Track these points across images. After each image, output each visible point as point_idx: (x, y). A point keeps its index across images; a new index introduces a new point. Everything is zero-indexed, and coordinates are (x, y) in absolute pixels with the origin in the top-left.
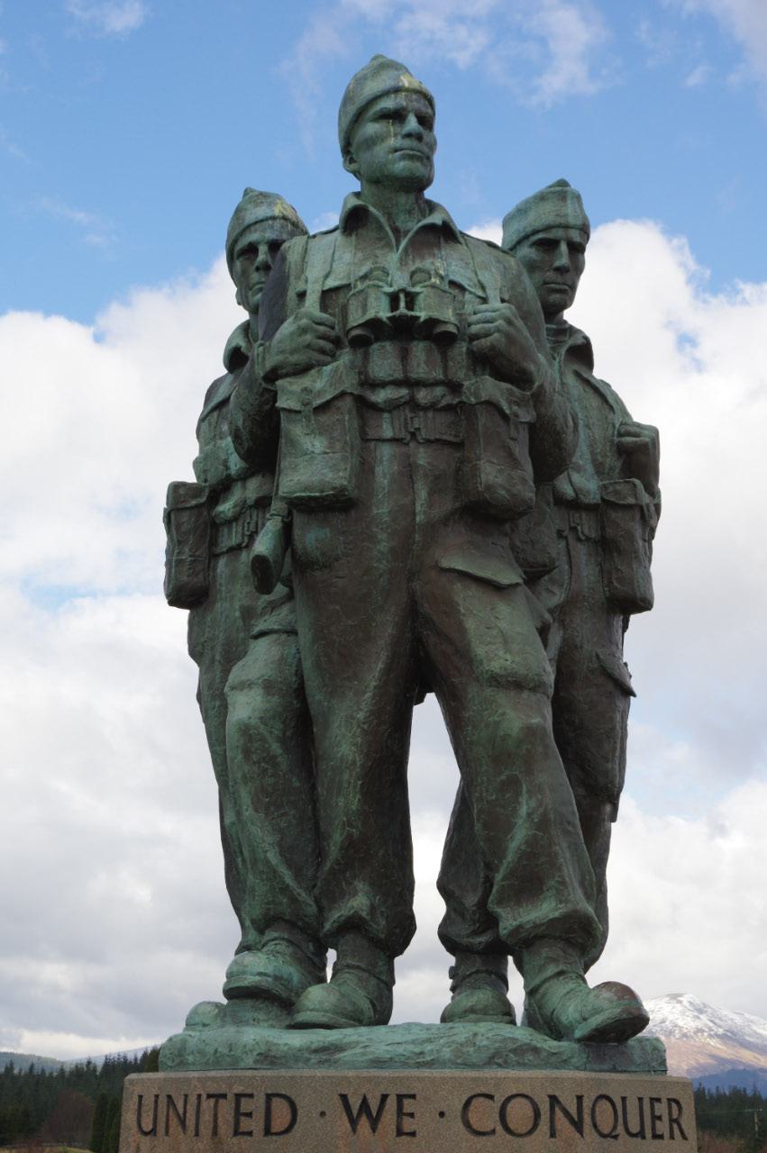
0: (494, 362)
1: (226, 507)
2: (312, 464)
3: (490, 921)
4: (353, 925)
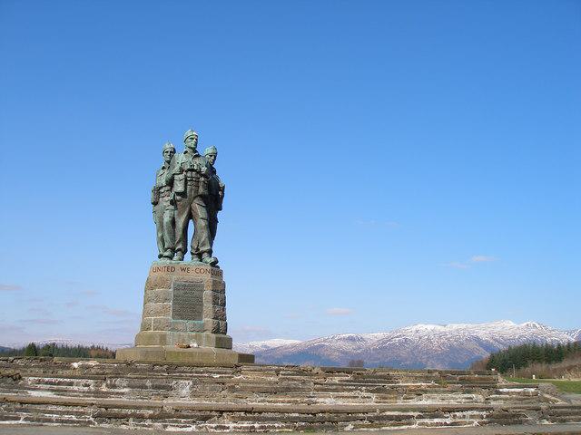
0: (205, 176)
1: (162, 190)
2: (179, 187)
3: (198, 249)
4: (179, 250)
